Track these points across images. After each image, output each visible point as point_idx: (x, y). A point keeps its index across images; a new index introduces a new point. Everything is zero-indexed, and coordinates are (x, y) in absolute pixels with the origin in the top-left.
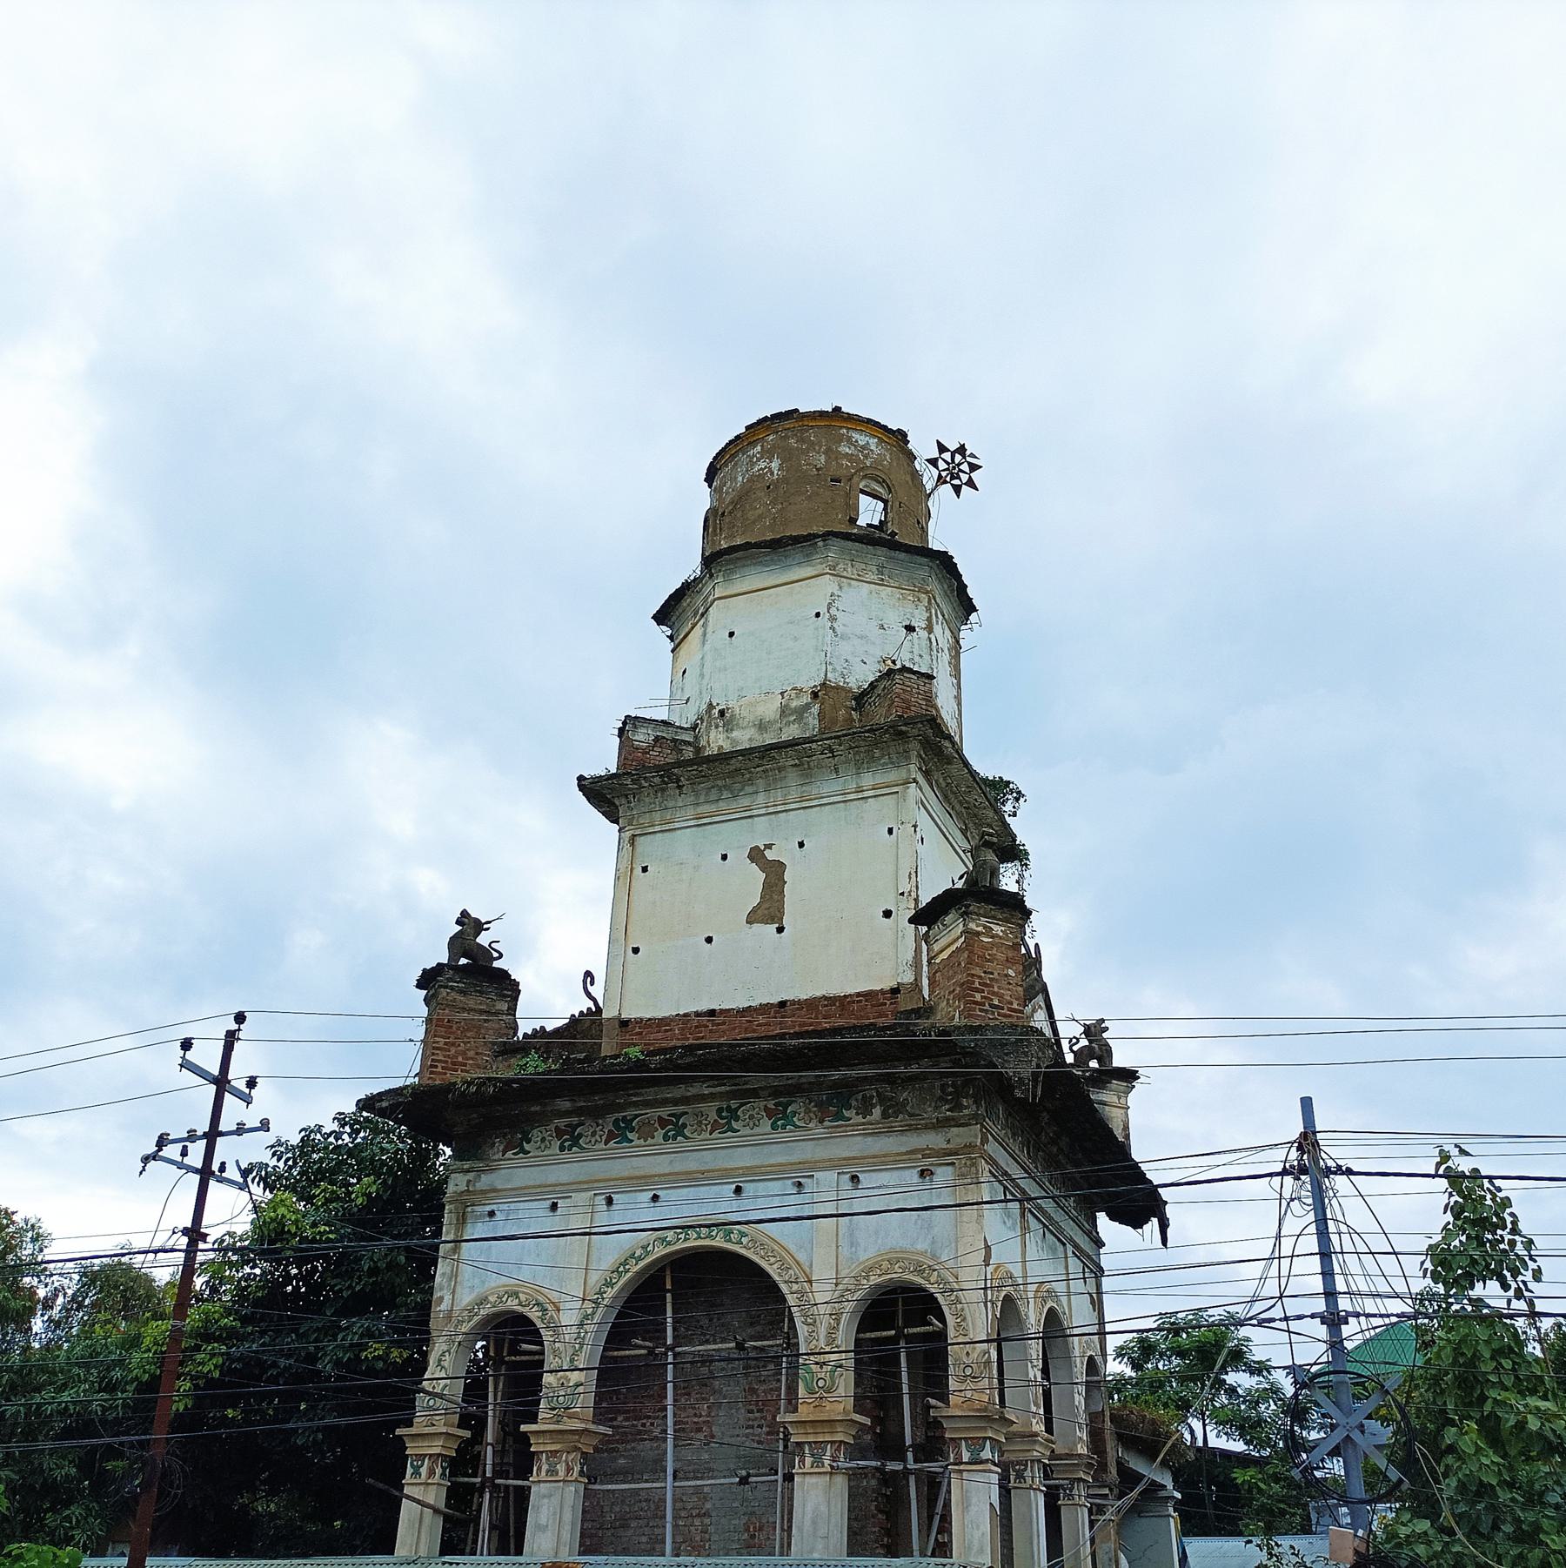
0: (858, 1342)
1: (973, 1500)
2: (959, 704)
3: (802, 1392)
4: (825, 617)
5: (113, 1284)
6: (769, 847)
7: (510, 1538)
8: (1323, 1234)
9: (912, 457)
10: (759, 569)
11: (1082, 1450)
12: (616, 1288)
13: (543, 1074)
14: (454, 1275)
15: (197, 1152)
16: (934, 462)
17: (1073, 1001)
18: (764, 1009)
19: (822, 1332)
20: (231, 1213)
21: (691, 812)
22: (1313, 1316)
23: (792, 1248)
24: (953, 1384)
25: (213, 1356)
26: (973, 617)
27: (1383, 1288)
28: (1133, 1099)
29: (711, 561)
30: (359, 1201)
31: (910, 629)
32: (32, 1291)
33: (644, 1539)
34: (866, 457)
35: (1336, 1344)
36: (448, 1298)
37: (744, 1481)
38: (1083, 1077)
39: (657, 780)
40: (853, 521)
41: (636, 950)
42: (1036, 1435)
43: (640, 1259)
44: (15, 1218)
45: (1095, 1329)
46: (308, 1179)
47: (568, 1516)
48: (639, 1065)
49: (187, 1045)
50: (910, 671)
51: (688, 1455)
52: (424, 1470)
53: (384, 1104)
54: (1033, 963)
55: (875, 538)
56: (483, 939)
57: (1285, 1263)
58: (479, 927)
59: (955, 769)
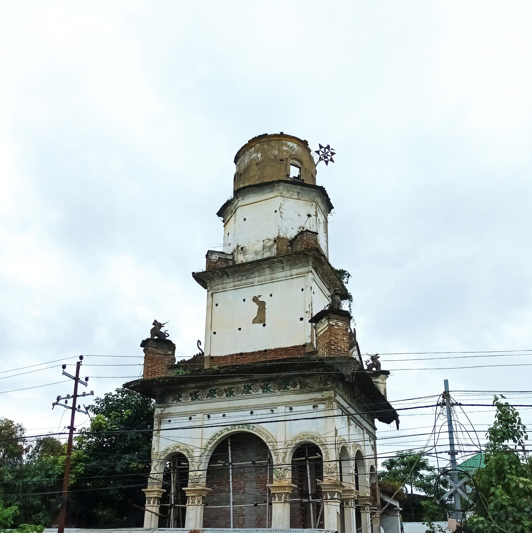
0: (293, 461)
1: (331, 511)
2: (327, 243)
3: (274, 477)
4: (278, 212)
5: (47, 444)
6: (260, 296)
7: (180, 523)
8: (450, 425)
9: (309, 151)
10: (254, 195)
11: (368, 495)
12: (212, 444)
13: (185, 375)
14: (158, 441)
15: (70, 402)
16: (318, 152)
17: (367, 349)
18: (260, 352)
19: (281, 459)
20: (84, 422)
22: (445, 452)
23: (270, 431)
24: (324, 475)
25: (81, 466)
26: (332, 211)
27: (470, 442)
28: (388, 381)
29: (238, 192)
30: (126, 417)
31: (309, 216)
32: (21, 447)
33: (224, 523)
34: (293, 151)
35: (453, 461)
36: (156, 448)
37: (256, 505)
38: (370, 374)
39: (220, 273)
40: (288, 175)
41: (215, 333)
42: (353, 490)
43: (220, 435)
44: (14, 423)
45: (373, 457)
46: (108, 410)
47: (199, 516)
48: (217, 372)
49: (64, 367)
50: (309, 231)
51: (237, 497)
52: (152, 502)
53: (132, 386)
54: (352, 335)
55: (297, 182)
56: (162, 330)
57: (437, 435)
58: (161, 326)
59: (325, 267)
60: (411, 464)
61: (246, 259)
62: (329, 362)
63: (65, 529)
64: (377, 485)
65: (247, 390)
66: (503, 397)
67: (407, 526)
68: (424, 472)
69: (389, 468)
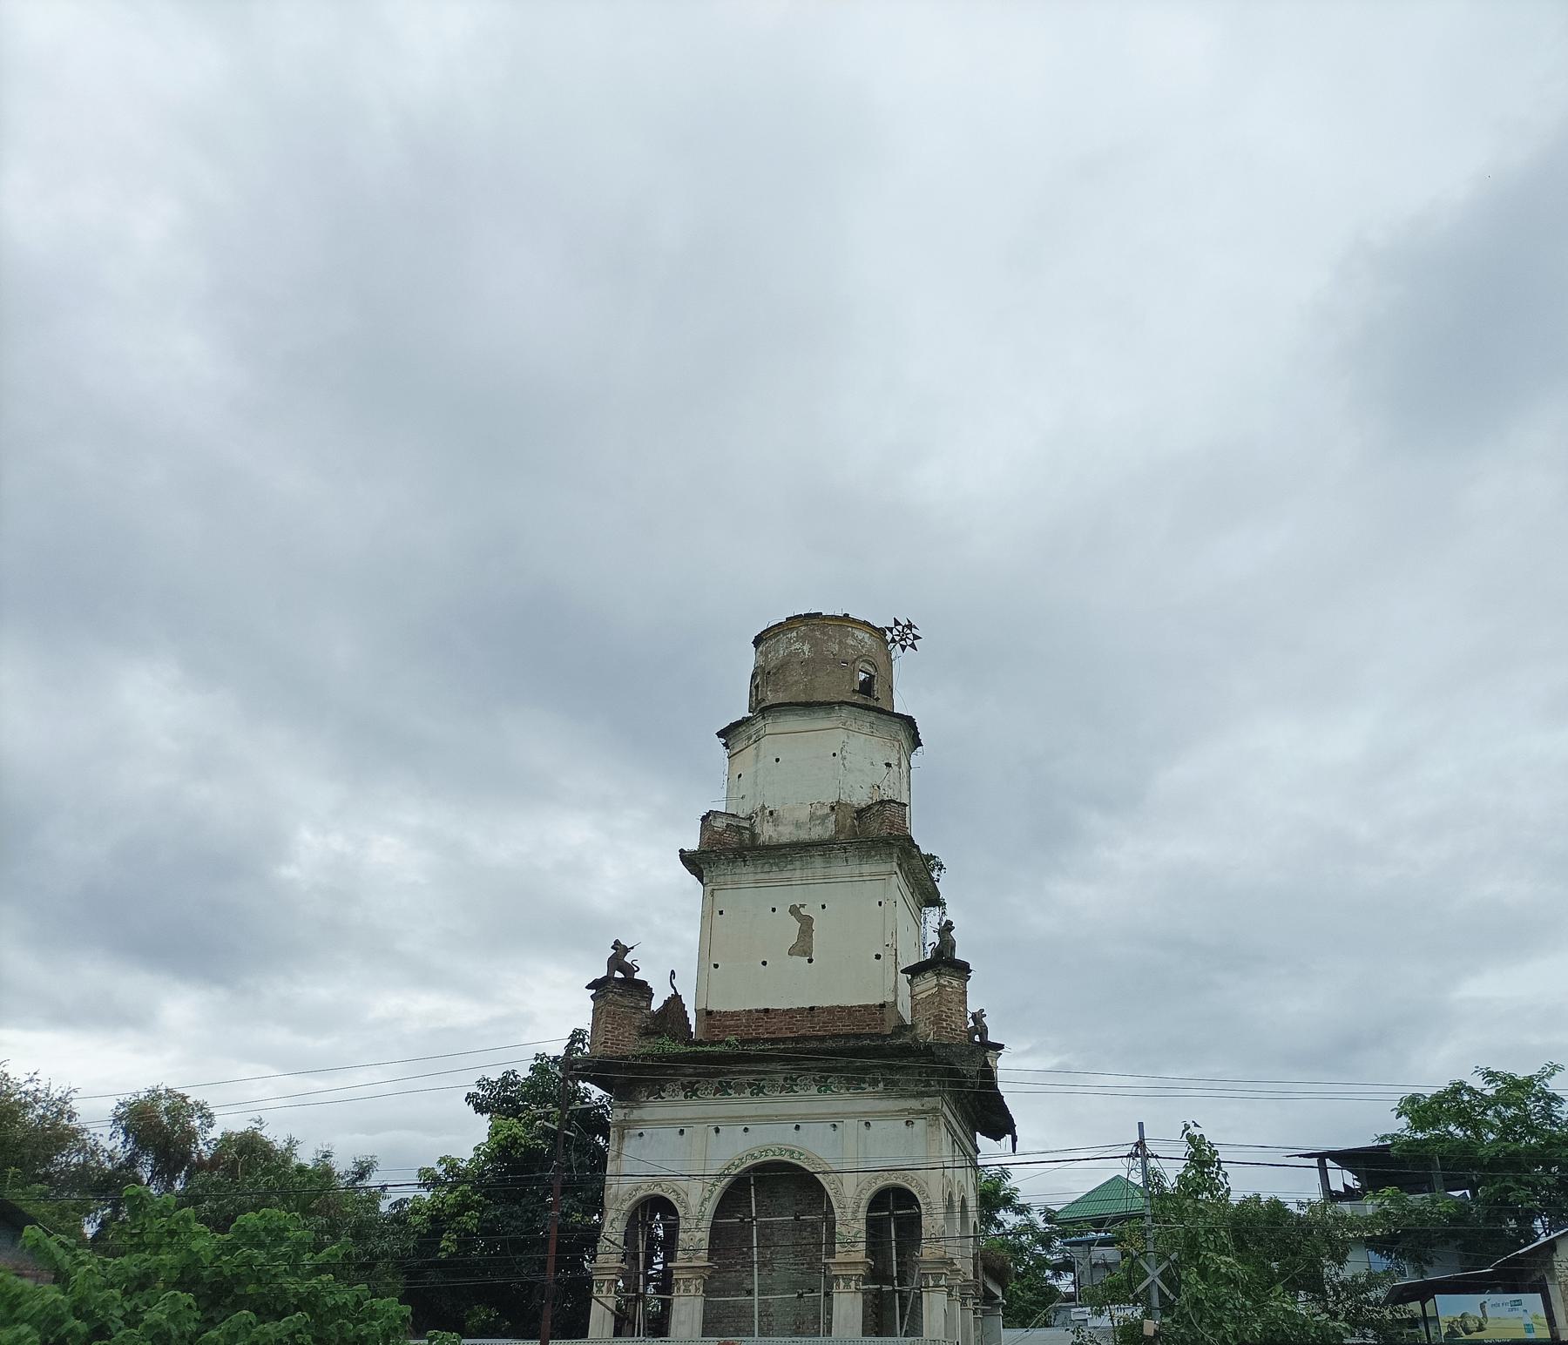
7: (659, 1326)
21: (751, 877)
31: (888, 765)
61: (780, 834)
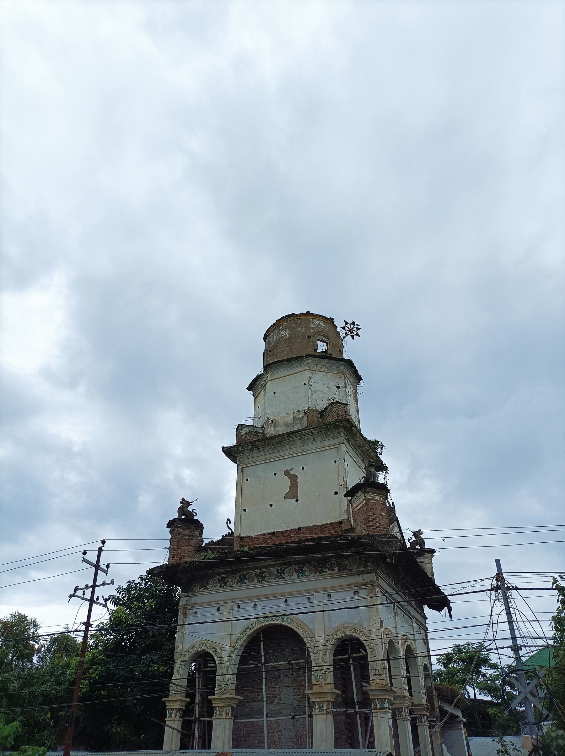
0: (334, 661)
1: (382, 724)
2: (358, 414)
3: (313, 681)
4: (307, 386)
5: (62, 641)
6: (291, 470)
7: (206, 743)
8: (509, 614)
9: (335, 327)
10: (283, 369)
11: (424, 702)
12: (242, 640)
13: (213, 559)
14: (183, 637)
15: (89, 592)
16: (344, 328)
17: (407, 526)
18: (293, 531)
19: (320, 656)
20: (101, 615)
21: (262, 458)
22: (507, 647)
23: (306, 623)
24: (372, 678)
26: (361, 382)
27: (535, 635)
28: (433, 560)
29: (266, 367)
30: (148, 609)
31: (338, 387)
32: (33, 646)
33: (256, 742)
34: (319, 328)
35: (518, 658)
36: (180, 646)
37: (293, 718)
38: (414, 552)
39: (250, 447)
40: (316, 350)
41: (245, 510)
42: (405, 697)
43: (251, 629)
44: (27, 618)
45: (426, 654)
46: (130, 601)
47: (227, 732)
48: (247, 554)
49: (85, 553)
50: (339, 403)
51: (272, 707)
52: (173, 715)
53: (156, 572)
54: (392, 509)
55: (324, 356)
56: (190, 509)
57: (495, 626)
58: (188, 504)
59: (358, 438)
60: (470, 660)
61: (277, 431)
62: (370, 540)
63: (72, 753)
64: (433, 689)
65: (280, 574)
66: (562, 578)
67: (475, 742)
68: (485, 670)
69: (446, 666)
